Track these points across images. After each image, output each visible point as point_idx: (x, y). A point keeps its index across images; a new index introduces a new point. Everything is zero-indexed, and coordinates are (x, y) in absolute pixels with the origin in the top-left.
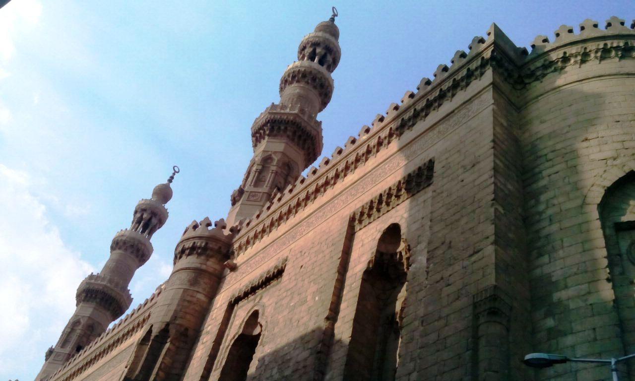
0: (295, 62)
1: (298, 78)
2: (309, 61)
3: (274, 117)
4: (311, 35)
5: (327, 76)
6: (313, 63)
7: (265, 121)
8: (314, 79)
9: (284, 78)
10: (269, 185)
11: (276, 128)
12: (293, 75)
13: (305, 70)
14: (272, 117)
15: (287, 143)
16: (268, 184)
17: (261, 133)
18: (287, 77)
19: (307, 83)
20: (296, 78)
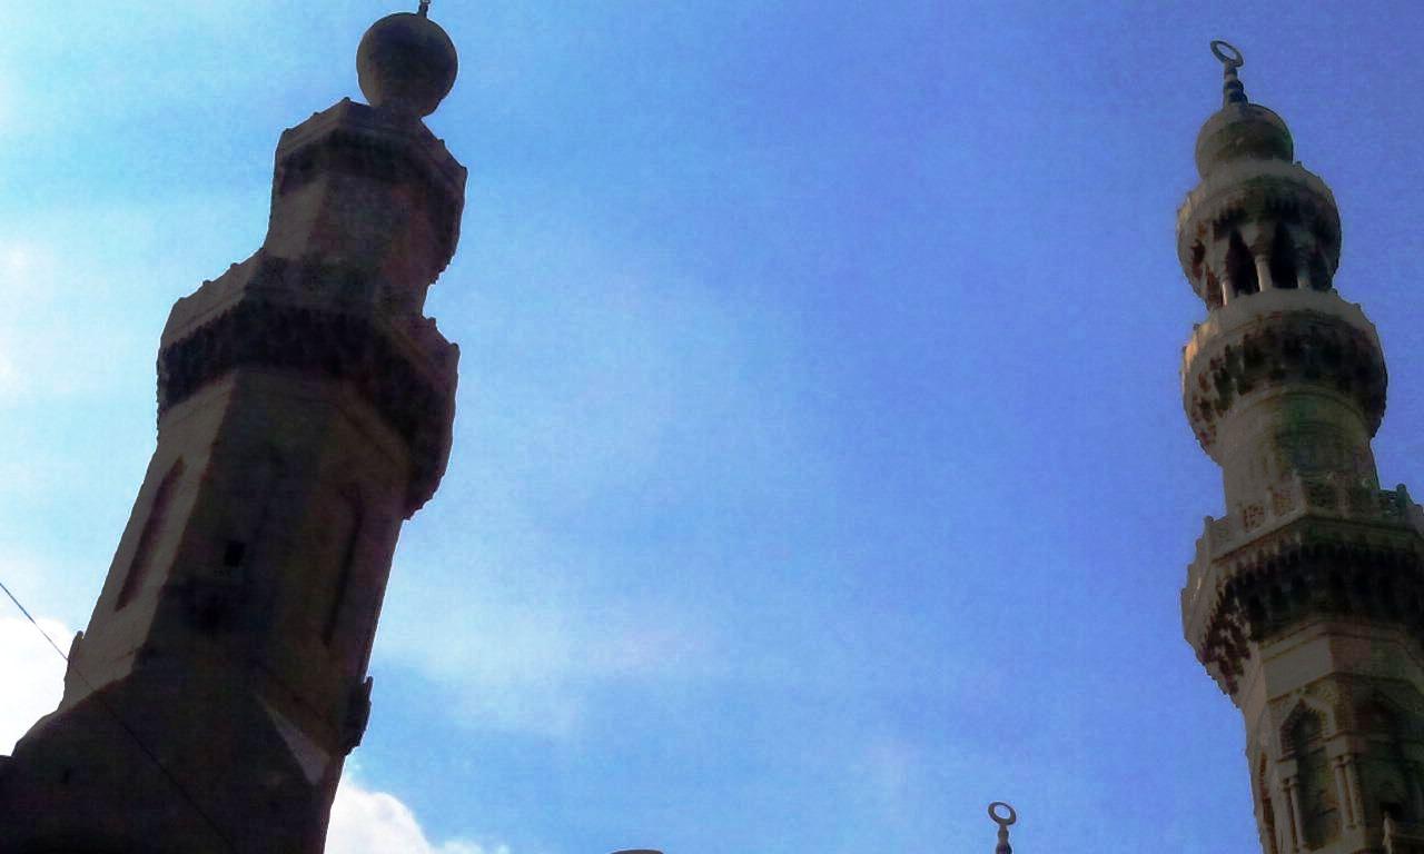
0: (1197, 327)
1: (1240, 377)
2: (1243, 297)
3: (1239, 565)
4: (1197, 198)
5: (1328, 311)
6: (1256, 295)
7: (1217, 598)
8: (1292, 350)
9: (1195, 398)
10: (1357, 818)
11: (1266, 600)
12: (1216, 377)
13: (1246, 337)
14: (1233, 571)
15: (1333, 633)
16: (1350, 813)
17: (1225, 642)
18: (1200, 393)
19: (1277, 376)
20: (1234, 380)
